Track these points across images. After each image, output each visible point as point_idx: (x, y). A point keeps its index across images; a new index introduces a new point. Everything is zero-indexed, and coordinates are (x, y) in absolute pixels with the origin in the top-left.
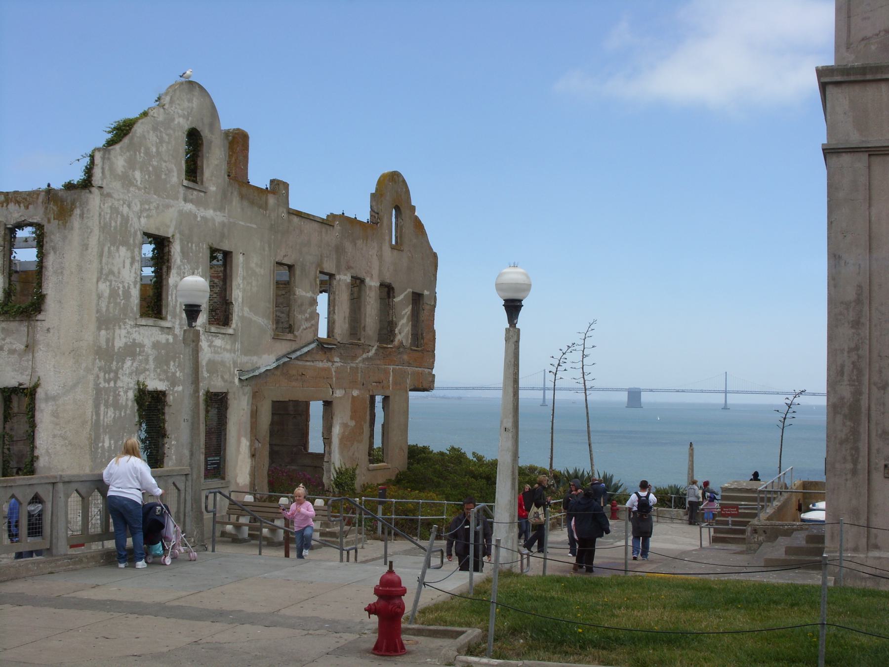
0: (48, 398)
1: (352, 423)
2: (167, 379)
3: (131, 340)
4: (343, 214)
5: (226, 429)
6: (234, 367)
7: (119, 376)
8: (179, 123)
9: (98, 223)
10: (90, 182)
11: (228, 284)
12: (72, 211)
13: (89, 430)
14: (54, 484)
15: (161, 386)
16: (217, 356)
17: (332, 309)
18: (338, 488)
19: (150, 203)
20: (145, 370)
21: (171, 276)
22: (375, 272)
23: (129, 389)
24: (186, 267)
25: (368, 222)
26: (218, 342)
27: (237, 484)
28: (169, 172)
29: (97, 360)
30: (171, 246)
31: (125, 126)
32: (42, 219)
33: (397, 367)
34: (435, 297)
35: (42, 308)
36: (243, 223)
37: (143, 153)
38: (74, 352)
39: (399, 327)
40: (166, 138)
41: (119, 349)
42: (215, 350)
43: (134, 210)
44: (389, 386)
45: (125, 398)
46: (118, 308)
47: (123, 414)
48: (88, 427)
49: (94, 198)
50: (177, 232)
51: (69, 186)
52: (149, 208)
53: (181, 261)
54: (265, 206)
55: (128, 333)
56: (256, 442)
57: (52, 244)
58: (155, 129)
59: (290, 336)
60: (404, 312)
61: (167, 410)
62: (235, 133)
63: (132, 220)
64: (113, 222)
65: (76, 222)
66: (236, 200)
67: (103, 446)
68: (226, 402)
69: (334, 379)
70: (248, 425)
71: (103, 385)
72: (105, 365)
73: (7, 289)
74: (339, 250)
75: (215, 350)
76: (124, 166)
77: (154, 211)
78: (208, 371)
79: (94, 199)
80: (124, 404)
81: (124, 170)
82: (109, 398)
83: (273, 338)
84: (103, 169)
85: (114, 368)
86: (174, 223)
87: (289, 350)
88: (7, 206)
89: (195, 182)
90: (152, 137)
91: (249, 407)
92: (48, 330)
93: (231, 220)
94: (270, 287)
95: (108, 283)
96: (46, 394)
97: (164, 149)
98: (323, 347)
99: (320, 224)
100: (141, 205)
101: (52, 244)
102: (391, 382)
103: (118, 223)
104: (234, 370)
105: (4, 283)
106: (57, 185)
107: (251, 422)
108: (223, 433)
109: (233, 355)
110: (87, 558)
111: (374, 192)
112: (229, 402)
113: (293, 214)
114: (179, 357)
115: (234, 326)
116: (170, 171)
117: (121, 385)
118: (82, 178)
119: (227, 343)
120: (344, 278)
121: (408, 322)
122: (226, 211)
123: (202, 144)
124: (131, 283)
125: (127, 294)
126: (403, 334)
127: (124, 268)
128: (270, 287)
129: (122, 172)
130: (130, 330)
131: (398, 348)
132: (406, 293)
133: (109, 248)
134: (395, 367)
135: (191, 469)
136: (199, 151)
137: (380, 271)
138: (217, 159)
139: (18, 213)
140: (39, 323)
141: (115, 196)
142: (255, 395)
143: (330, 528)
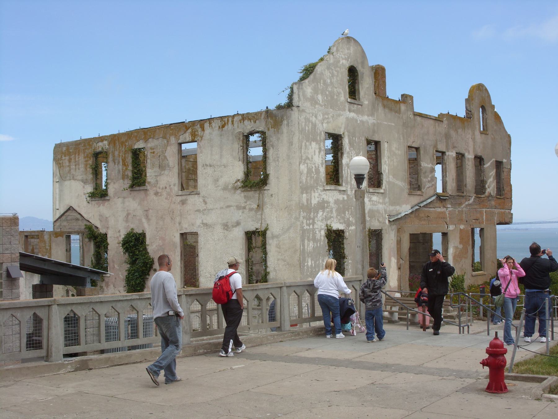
0: (273, 237)
1: (461, 246)
2: (345, 222)
3: (322, 199)
4: (448, 113)
5: (382, 252)
6: (385, 214)
7: (315, 221)
8: (343, 63)
9: (298, 129)
10: (292, 104)
11: (379, 161)
12: (282, 122)
13: (298, 255)
14: (281, 287)
15: (341, 227)
16: (374, 207)
17: (444, 174)
18: (453, 288)
19: (328, 114)
20: (331, 217)
21: (344, 158)
22: (471, 149)
23: (322, 229)
24: (352, 152)
25: (465, 117)
26: (375, 198)
27: (390, 287)
28: (339, 94)
29: (302, 212)
30: (342, 140)
31: (310, 68)
32: (265, 129)
33: (488, 209)
34: (511, 163)
35: (267, 182)
36: (386, 123)
37: (322, 84)
38: (287, 208)
39: (488, 184)
40: (335, 73)
41: (314, 205)
42: (373, 203)
43: (319, 119)
44: (483, 222)
45: (319, 235)
46: (312, 180)
47: (318, 245)
48: (298, 254)
49: (295, 114)
50: (346, 130)
51: (279, 107)
52: (328, 117)
53: (349, 149)
54: (399, 111)
55: (319, 195)
56: (401, 259)
57: (271, 143)
58: (328, 68)
59: (419, 193)
60: (491, 174)
61: (345, 241)
62: (377, 68)
63: (318, 125)
64: (307, 127)
65: (284, 129)
66: (380, 108)
67: (308, 264)
68: (381, 236)
69: (448, 219)
70: (396, 249)
71: (306, 227)
72: (307, 215)
73: (246, 172)
74: (447, 136)
75: (373, 203)
76: (311, 93)
77: (331, 119)
78: (369, 217)
79: (294, 114)
80: (319, 238)
81: (311, 95)
82: (310, 235)
83: (408, 194)
84: (299, 95)
85: (312, 217)
86: (343, 125)
87: (419, 201)
88: (243, 122)
89: (355, 99)
90: (327, 73)
91: (396, 238)
92: (272, 195)
93: (379, 121)
94: (405, 162)
95: (306, 165)
96: (272, 234)
97: (334, 80)
98: (440, 198)
99: (434, 120)
100: (323, 116)
101: (271, 143)
102: (484, 219)
103: (310, 127)
104: (385, 215)
105: (244, 169)
106: (272, 107)
107: (397, 248)
108: (380, 255)
109: (384, 206)
110: (302, 333)
111: (467, 98)
112: (383, 235)
113: (417, 115)
114: (351, 208)
115: (384, 187)
116: (339, 93)
117: (317, 227)
118: (287, 102)
119: (380, 198)
120: (451, 154)
121: (493, 180)
122: (375, 116)
123: (358, 75)
124: (319, 164)
125: (317, 171)
126: (491, 188)
127: (315, 155)
128: (405, 162)
129: (310, 96)
130: (320, 193)
131: (488, 197)
132: (491, 161)
133: (305, 143)
134: (487, 209)
135: (364, 277)
136: (356, 79)
137: (474, 148)
138: (368, 84)
139: (250, 126)
140: (266, 192)
141: (307, 111)
142: (399, 231)
143: (449, 313)
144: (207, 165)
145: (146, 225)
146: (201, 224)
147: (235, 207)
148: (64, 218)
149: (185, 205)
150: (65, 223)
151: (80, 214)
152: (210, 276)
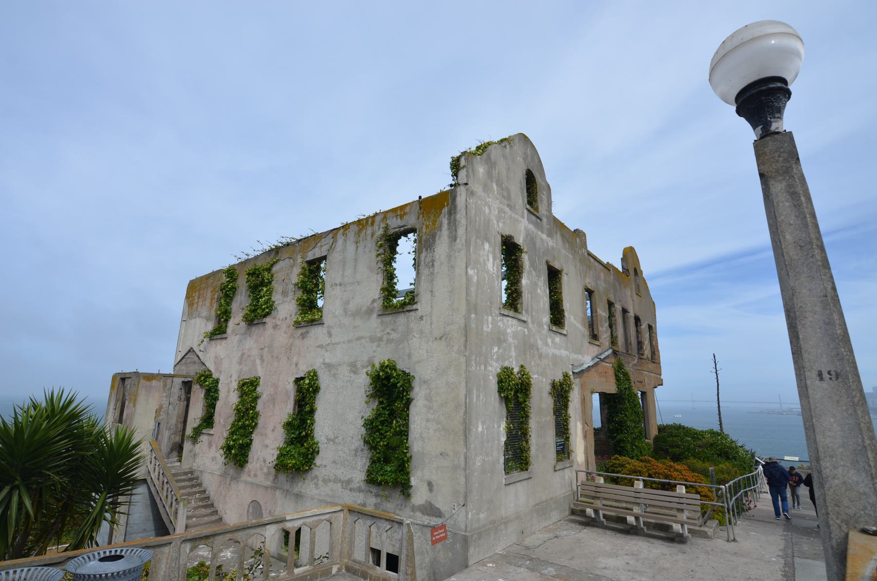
70: (580, 411)
83: (589, 342)
91: (580, 396)
92: (421, 318)
115: (566, 328)
122: (554, 240)
127: (488, 260)
132: (645, 324)
144: (336, 285)
145: (259, 368)
146: (322, 365)
147: (367, 339)
148: (183, 361)
149: (305, 340)
150: (184, 368)
151: (198, 356)
152: (326, 441)
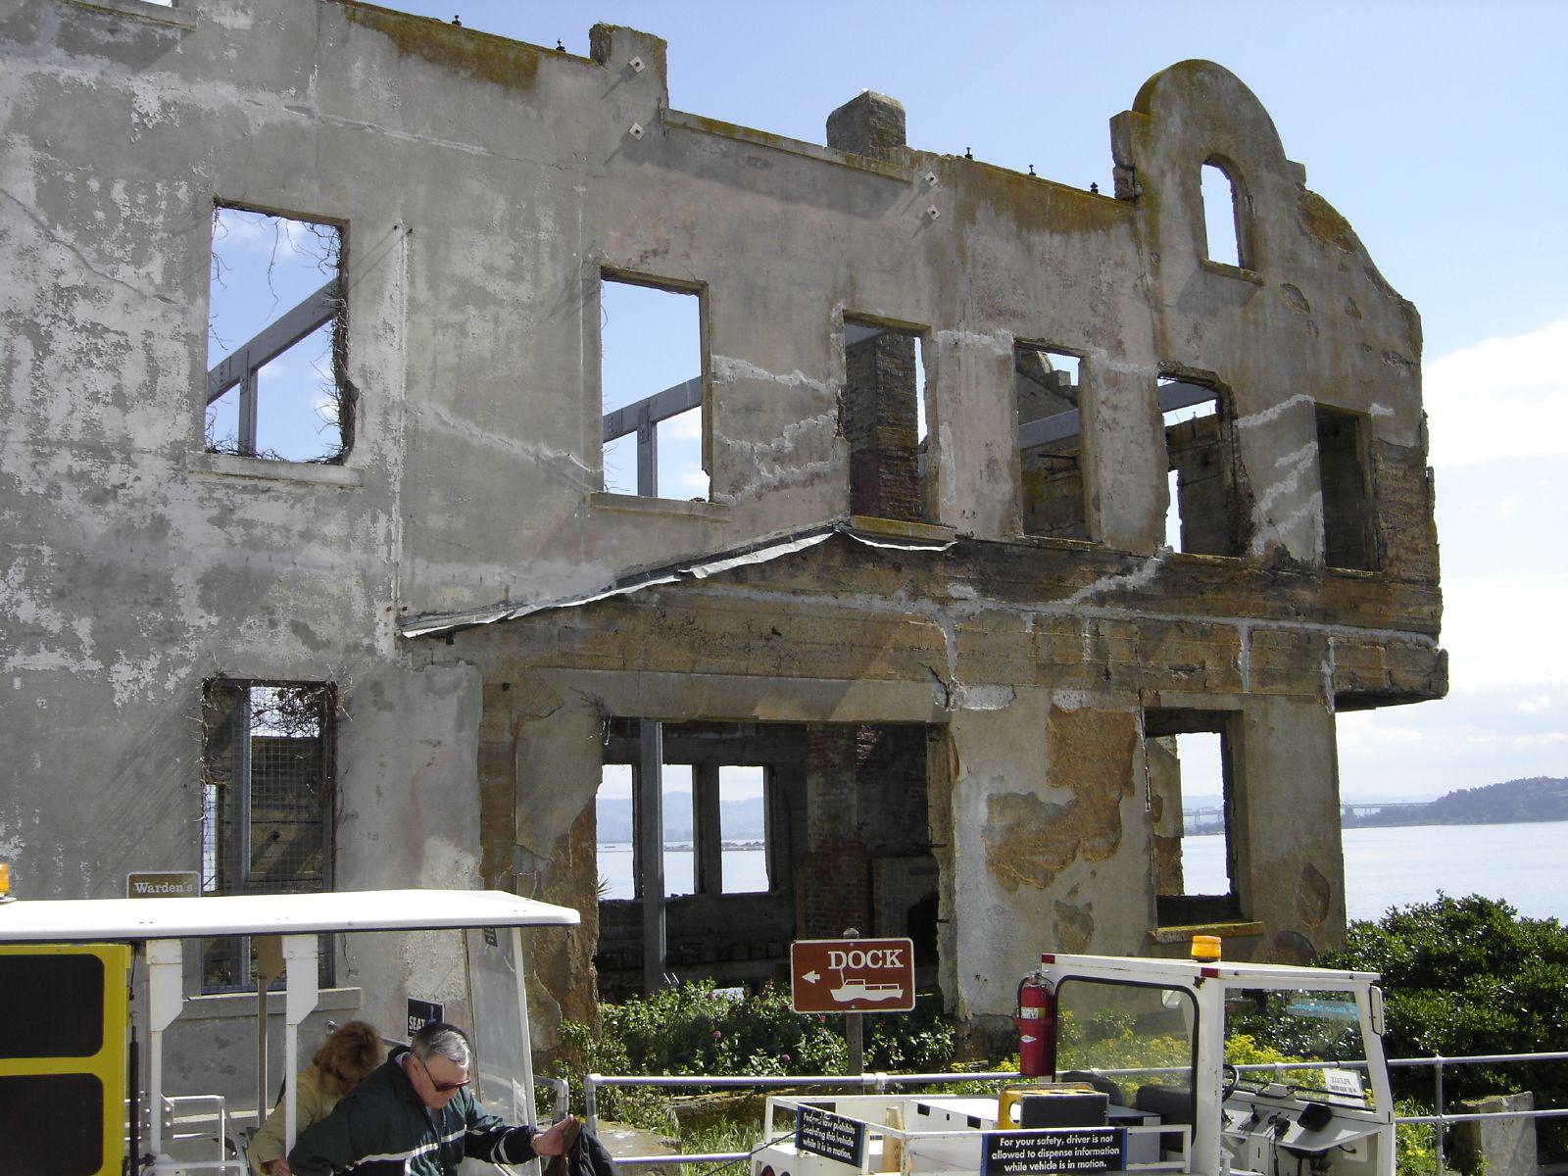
132: (1284, 405)
